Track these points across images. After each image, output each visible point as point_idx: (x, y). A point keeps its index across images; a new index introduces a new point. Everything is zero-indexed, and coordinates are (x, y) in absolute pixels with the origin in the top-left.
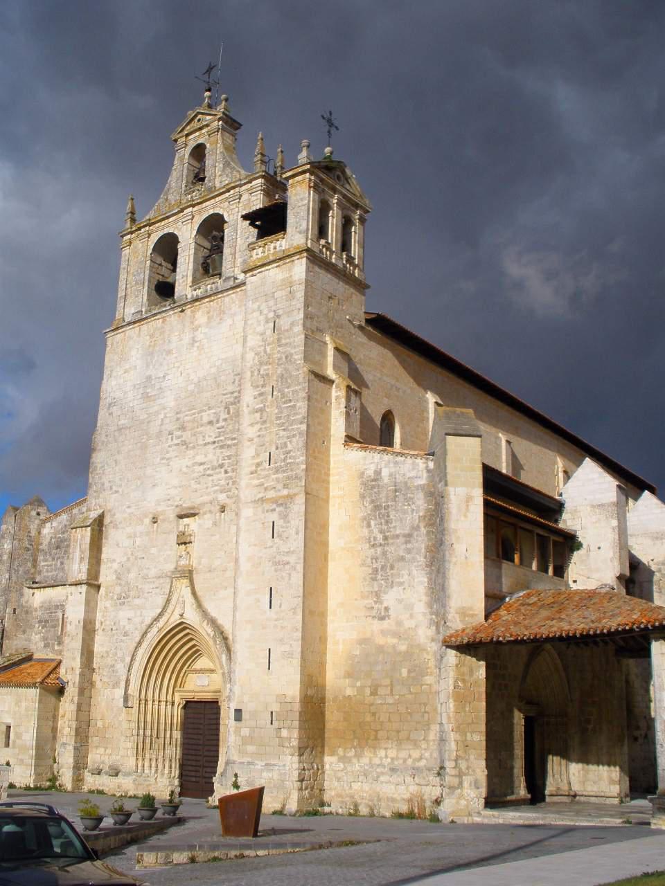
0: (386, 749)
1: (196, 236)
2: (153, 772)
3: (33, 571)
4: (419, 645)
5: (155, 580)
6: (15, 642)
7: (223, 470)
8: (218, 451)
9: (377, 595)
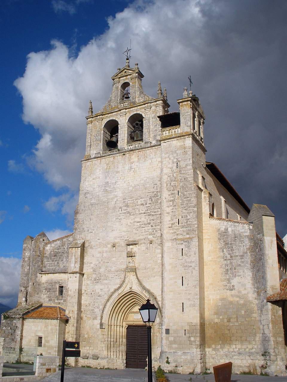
0: (235, 344)
1: (127, 122)
2: (115, 357)
4: (249, 301)
6: (34, 298)
7: (150, 225)
8: (147, 217)
9: (229, 280)
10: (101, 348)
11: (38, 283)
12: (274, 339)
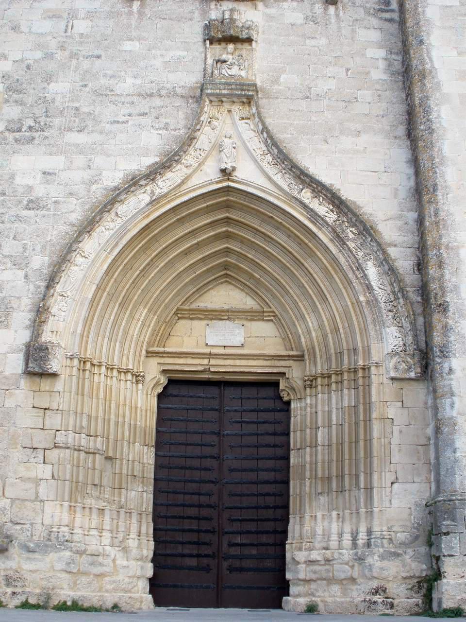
5: (135, 99)
10: (29, 485)
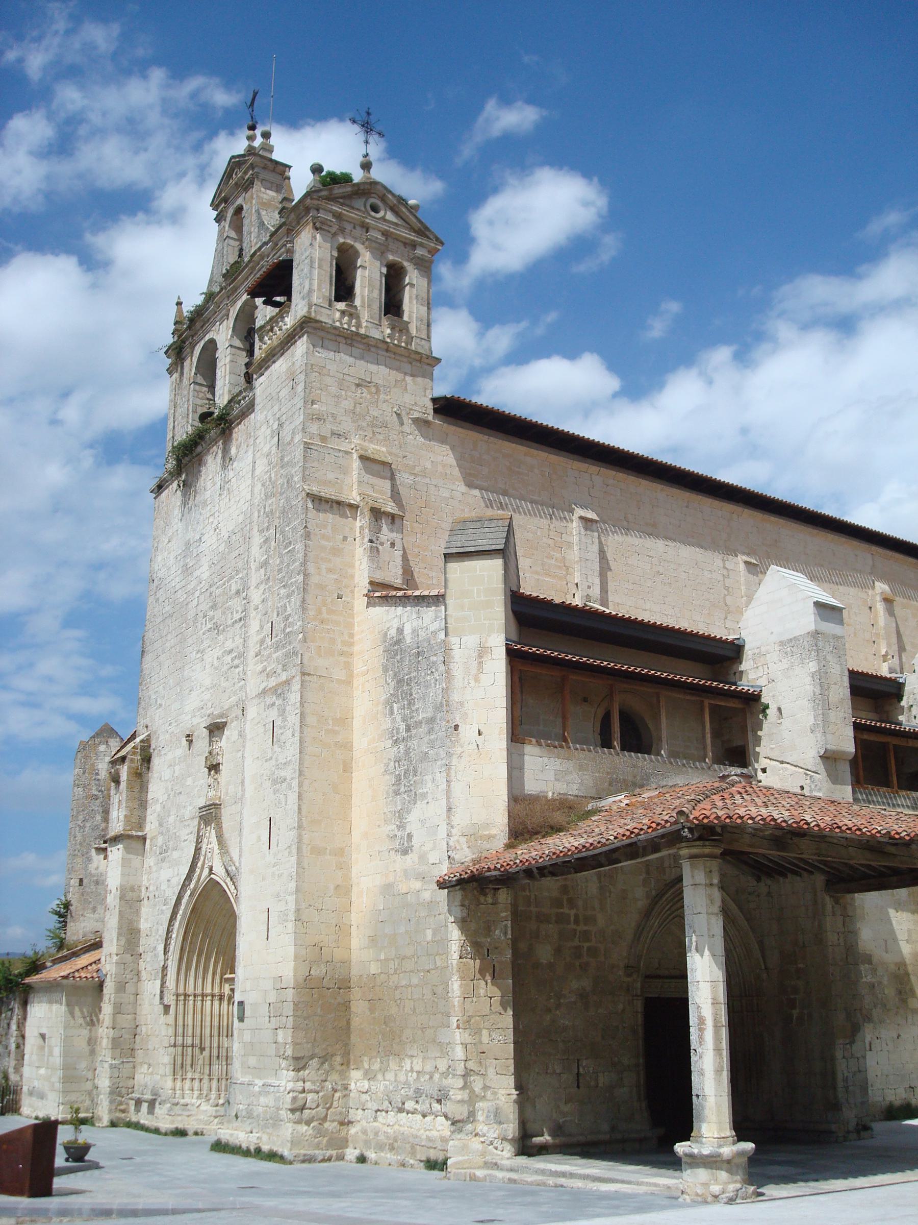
3: (103, 825)
6: (83, 925)
9: (400, 816)
11: (95, 878)
12: (469, 1039)
